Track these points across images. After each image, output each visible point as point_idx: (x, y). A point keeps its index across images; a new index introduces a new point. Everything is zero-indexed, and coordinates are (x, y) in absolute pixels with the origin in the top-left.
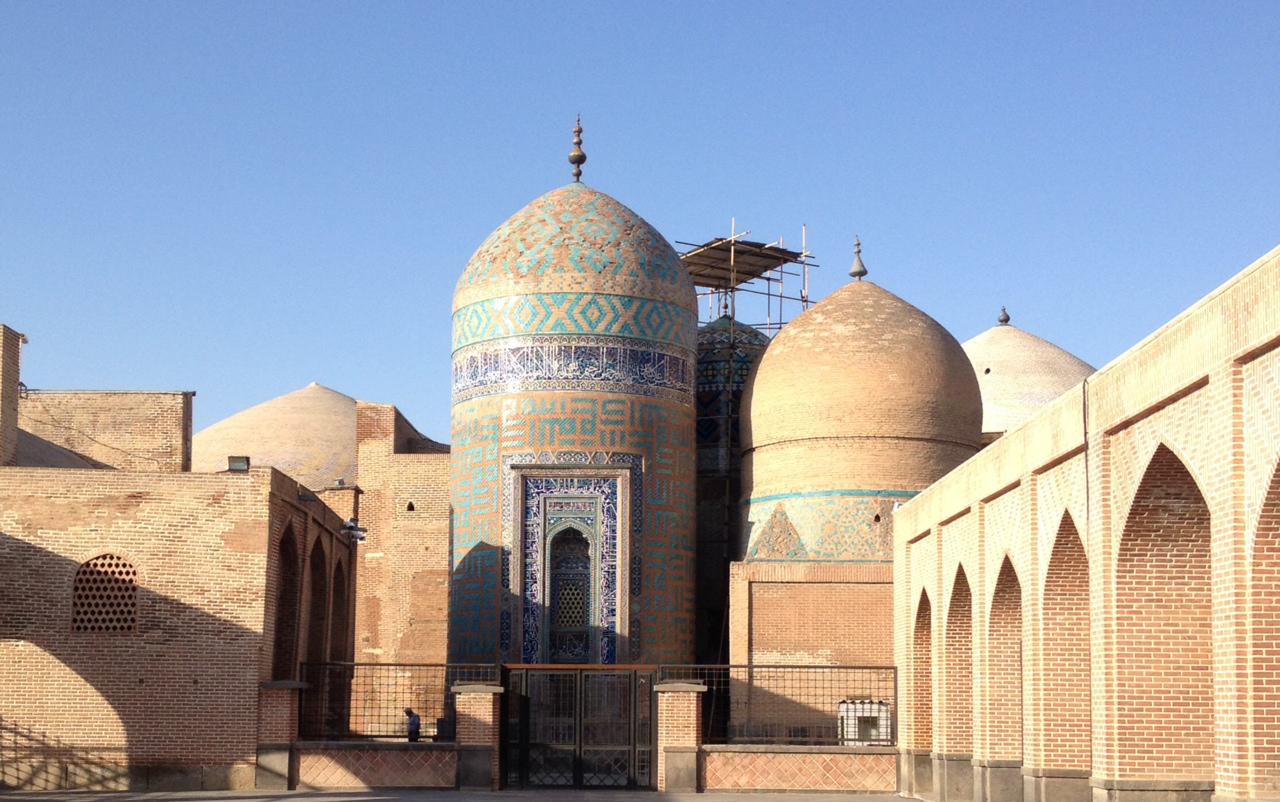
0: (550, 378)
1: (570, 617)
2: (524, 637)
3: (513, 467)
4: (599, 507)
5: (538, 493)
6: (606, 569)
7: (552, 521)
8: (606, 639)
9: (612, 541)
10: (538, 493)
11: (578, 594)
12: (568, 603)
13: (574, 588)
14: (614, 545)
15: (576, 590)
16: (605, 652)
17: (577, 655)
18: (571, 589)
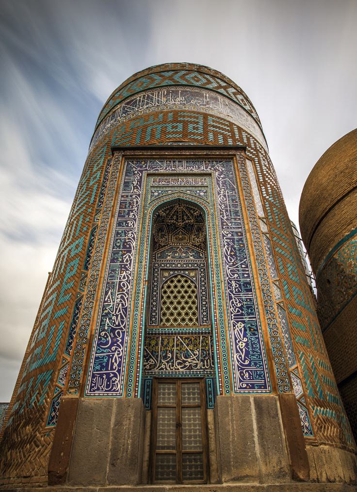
0: (157, 106)
1: (179, 314)
2: (102, 324)
3: (114, 149)
4: (214, 181)
5: (141, 171)
6: (229, 235)
7: (156, 194)
8: (241, 325)
9: (232, 209)
10: (141, 171)
11: (189, 287)
12: (175, 297)
13: (183, 280)
14: (236, 213)
15: (186, 281)
16: (242, 345)
17: (190, 368)
18: (179, 281)
